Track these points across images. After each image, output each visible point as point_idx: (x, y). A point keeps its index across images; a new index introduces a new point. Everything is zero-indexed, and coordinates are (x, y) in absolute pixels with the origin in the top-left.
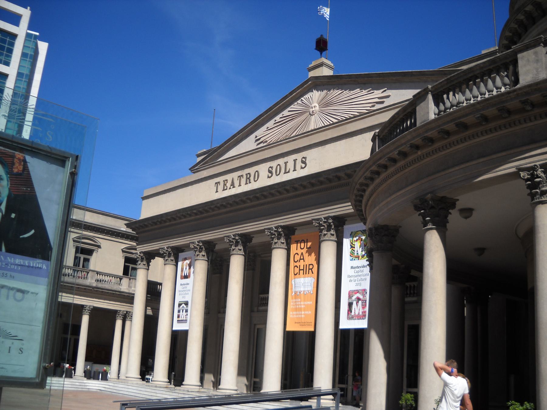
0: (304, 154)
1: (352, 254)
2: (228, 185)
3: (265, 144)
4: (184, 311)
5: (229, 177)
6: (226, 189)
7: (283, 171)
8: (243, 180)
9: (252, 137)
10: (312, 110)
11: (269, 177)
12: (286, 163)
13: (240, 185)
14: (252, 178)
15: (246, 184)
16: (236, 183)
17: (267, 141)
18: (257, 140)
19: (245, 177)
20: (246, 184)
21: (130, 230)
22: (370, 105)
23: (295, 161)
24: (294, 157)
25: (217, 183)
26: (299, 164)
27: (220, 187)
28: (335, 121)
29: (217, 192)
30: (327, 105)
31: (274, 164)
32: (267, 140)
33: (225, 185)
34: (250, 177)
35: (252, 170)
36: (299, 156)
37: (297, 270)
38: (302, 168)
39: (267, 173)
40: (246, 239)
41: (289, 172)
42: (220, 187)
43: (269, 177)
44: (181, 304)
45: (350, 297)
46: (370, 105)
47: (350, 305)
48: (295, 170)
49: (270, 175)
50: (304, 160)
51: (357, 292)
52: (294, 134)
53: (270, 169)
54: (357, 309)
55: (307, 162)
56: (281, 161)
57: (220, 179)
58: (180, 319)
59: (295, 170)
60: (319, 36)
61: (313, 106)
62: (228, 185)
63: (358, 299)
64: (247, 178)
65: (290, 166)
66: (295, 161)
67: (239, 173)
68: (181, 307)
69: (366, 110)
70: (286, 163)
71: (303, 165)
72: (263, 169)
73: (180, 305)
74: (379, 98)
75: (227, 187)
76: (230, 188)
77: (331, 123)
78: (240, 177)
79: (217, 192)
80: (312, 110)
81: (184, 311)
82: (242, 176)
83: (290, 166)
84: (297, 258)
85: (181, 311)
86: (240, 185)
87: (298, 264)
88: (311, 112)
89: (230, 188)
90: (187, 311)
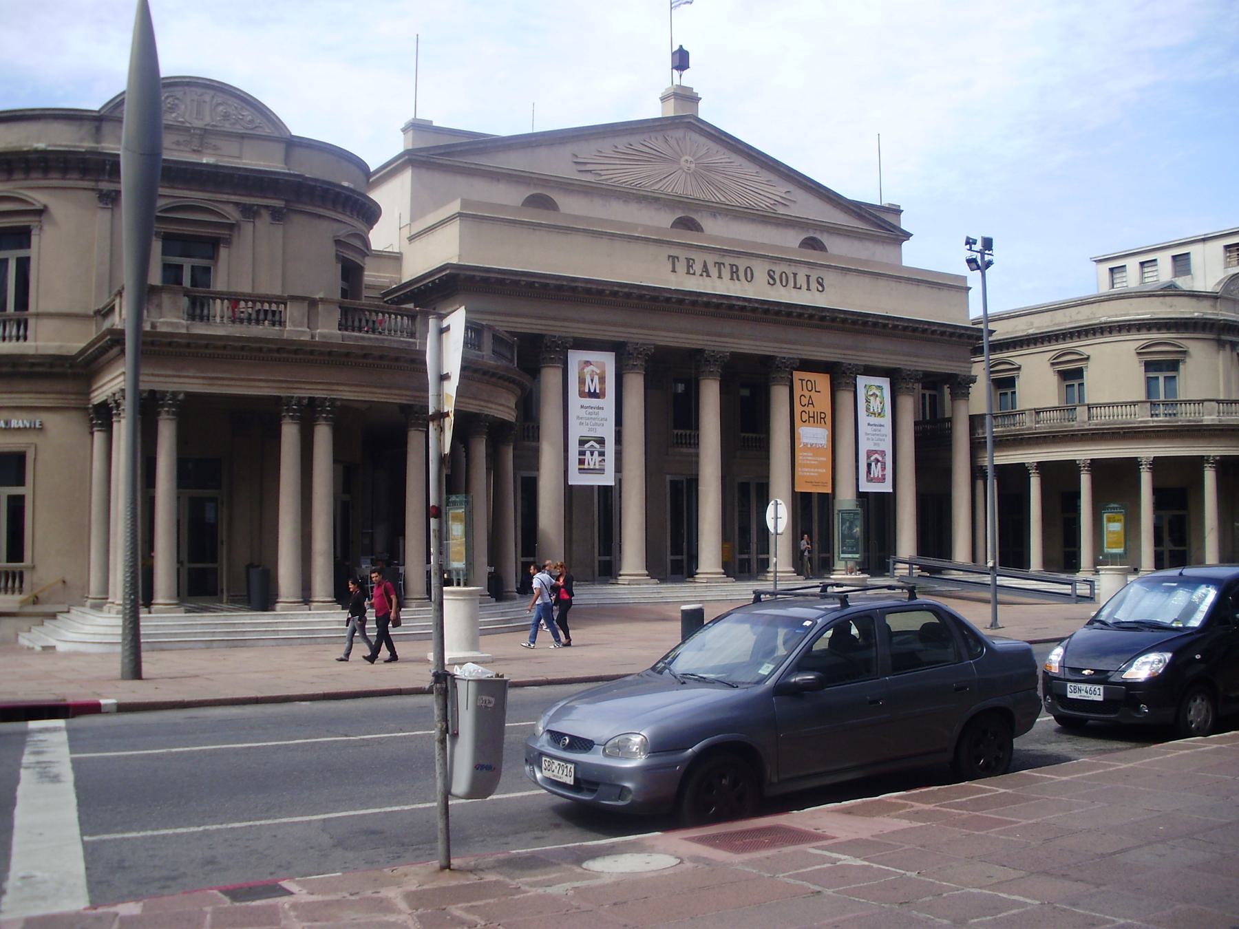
1: (868, 409)
2: (698, 268)
4: (596, 453)
5: (699, 259)
8: (726, 273)
9: (567, 151)
12: (795, 275)
13: (720, 277)
15: (732, 279)
16: (714, 272)
19: (728, 267)
20: (732, 279)
23: (808, 277)
26: (814, 285)
27: (681, 267)
29: (674, 271)
31: (778, 269)
33: (689, 267)
35: (742, 263)
37: (805, 417)
44: (588, 441)
45: (869, 457)
47: (869, 465)
48: (808, 289)
51: (876, 452)
54: (876, 471)
56: (784, 267)
57: (682, 254)
58: (586, 466)
59: (808, 289)
61: (690, 159)
62: (698, 268)
63: (878, 461)
64: (732, 273)
65: (801, 280)
66: (808, 277)
68: (587, 446)
70: (795, 275)
72: (760, 270)
73: (582, 442)
79: (674, 271)
81: (596, 453)
83: (801, 280)
84: (805, 401)
85: (588, 453)
86: (720, 277)
87: (805, 409)
90: (602, 454)
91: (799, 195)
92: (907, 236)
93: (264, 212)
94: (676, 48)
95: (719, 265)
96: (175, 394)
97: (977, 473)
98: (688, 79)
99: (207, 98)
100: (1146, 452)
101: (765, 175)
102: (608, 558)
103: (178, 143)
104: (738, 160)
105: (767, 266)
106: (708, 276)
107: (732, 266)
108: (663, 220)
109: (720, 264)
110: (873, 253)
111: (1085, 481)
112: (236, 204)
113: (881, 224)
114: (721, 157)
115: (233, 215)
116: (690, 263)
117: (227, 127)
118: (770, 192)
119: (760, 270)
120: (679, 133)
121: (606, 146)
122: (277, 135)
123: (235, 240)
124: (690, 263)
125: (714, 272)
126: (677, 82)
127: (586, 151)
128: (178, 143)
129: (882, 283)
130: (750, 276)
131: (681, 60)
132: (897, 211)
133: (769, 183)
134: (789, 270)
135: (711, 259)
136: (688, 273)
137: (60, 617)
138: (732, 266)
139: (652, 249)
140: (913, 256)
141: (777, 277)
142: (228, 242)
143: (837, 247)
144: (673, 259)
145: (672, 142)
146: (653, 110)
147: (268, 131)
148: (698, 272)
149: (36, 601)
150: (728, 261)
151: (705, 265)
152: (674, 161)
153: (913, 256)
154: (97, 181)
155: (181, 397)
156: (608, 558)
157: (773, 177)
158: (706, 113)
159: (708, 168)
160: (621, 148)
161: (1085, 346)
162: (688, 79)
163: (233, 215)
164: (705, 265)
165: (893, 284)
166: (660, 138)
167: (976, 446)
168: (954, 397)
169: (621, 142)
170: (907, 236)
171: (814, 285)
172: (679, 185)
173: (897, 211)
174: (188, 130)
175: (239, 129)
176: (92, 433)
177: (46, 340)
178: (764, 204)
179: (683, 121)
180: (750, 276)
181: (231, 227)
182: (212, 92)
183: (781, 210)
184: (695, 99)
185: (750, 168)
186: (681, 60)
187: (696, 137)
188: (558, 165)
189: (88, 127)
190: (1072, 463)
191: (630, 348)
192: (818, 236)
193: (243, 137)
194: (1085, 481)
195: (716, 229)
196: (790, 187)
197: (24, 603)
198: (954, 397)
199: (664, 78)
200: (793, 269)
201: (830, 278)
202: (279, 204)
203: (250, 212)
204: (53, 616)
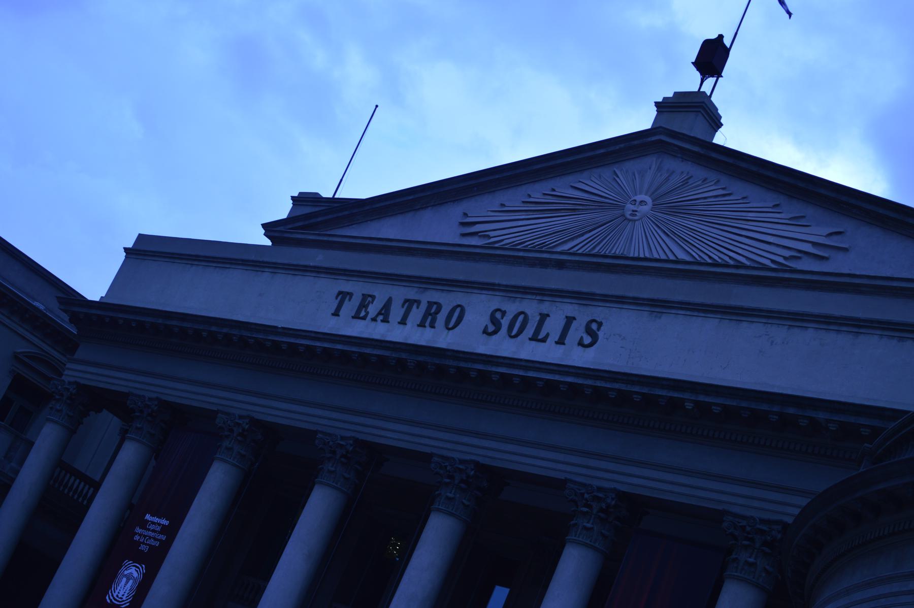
0: (599, 312)
2: (373, 309)
5: (381, 292)
6: (364, 318)
7: (530, 331)
8: (416, 314)
9: (455, 212)
10: (633, 207)
11: (485, 332)
13: (403, 322)
14: (441, 318)
15: (422, 325)
16: (396, 312)
17: (489, 237)
18: (463, 224)
19: (424, 306)
20: (422, 325)
21: (66, 317)
22: (787, 253)
23: (570, 320)
24: (569, 309)
25: (344, 296)
26: (577, 332)
27: (349, 307)
28: (682, 256)
29: (336, 314)
30: (675, 209)
31: (512, 308)
32: (492, 234)
33: (363, 305)
34: (438, 311)
35: (447, 300)
36: (583, 315)
38: (581, 344)
39: (485, 320)
40: (369, 456)
41: (543, 340)
42: (349, 307)
43: (485, 332)
46: (787, 253)
48: (561, 342)
49: (491, 328)
50: (594, 326)
52: (566, 247)
53: (498, 315)
55: (601, 334)
57: (357, 288)
59: (561, 342)
60: (714, 36)
61: (639, 198)
62: (373, 309)
64: (427, 313)
65: (553, 326)
66: (570, 320)
67: (411, 293)
69: (773, 261)
70: (544, 317)
71: (587, 340)
72: (479, 309)
74: (814, 244)
75: (367, 313)
76: (374, 320)
77: (672, 258)
78: (410, 304)
80: (633, 207)
82: (418, 302)
83: (553, 326)
88: (628, 214)
89: (374, 320)
95: (410, 304)
105: (493, 302)
106: (386, 320)
107: (430, 304)
133: (796, 221)
134: (532, 308)
135: (399, 293)
136: (356, 317)
138: (430, 304)
141: (505, 322)
144: (344, 296)
151: (389, 303)
160: (537, 196)
164: (389, 303)
165: (778, 332)
169: (537, 191)
171: (577, 332)
185: (760, 199)
186: (712, 57)
200: (545, 308)
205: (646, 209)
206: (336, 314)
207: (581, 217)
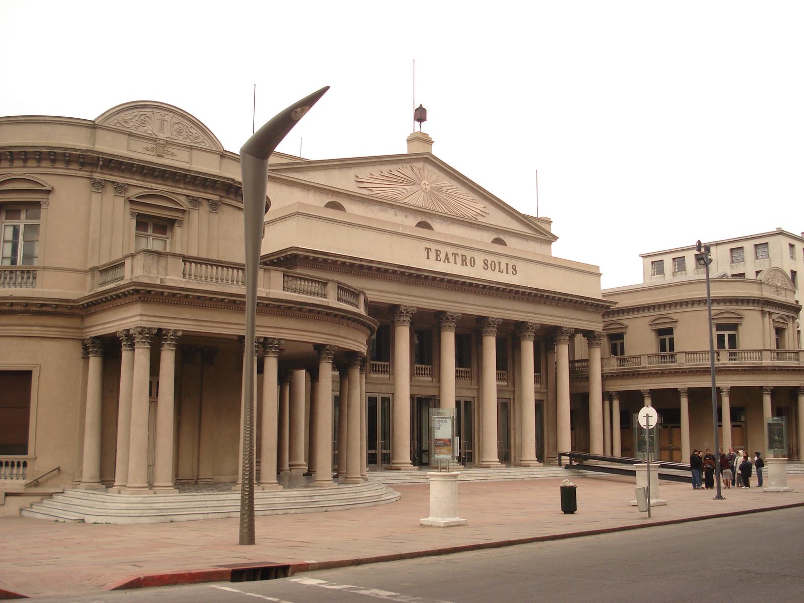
2: (442, 256)
3: (371, 193)
5: (443, 250)
8: (459, 260)
9: (352, 173)
12: (500, 263)
13: (455, 263)
14: (468, 261)
16: (452, 259)
23: (507, 264)
26: (510, 270)
27: (433, 255)
29: (428, 258)
31: (490, 258)
33: (437, 256)
35: (469, 254)
36: (511, 262)
52: (406, 201)
61: (427, 183)
62: (442, 256)
65: (503, 267)
70: (500, 263)
72: (479, 259)
83: (503, 267)
86: (455, 263)
91: (491, 209)
92: (555, 238)
93: (205, 202)
94: (417, 106)
95: (455, 255)
96: (176, 331)
97: (607, 396)
98: (426, 127)
99: (167, 118)
100: (726, 383)
101: (471, 196)
102: (373, 452)
103: (147, 149)
104: (455, 185)
108: (411, 221)
109: (455, 255)
110: (533, 249)
111: (684, 402)
112: (188, 196)
113: (539, 231)
114: (445, 181)
115: (185, 204)
116: (438, 253)
117: (180, 140)
118: (474, 207)
119: (479, 259)
120: (420, 165)
121: (376, 171)
122: (214, 149)
123: (185, 222)
124: (438, 253)
125: (452, 259)
126: (417, 129)
127: (364, 173)
128: (147, 149)
129: (550, 270)
130: (473, 263)
131: (420, 115)
132: (549, 222)
134: (496, 259)
135: (450, 250)
137: (54, 496)
139: (415, 242)
140: (558, 250)
141: (489, 264)
142: (181, 223)
143: (513, 244)
144: (428, 250)
145: (416, 170)
146: (402, 148)
147: (208, 145)
148: (443, 259)
149: (36, 483)
150: (460, 252)
152: (417, 183)
153: (558, 250)
154: (91, 172)
155: (180, 334)
156: (373, 452)
157: (476, 197)
158: (437, 151)
159: (438, 190)
161: (674, 313)
162: (426, 127)
163: (185, 204)
166: (409, 167)
167: (605, 378)
168: (590, 345)
170: (555, 238)
172: (418, 199)
173: (549, 222)
174: (155, 140)
175: (188, 142)
176: (86, 358)
177: (50, 287)
178: (469, 214)
179: (420, 156)
180: (473, 263)
181: (183, 211)
182: (172, 115)
183: (480, 219)
184: (430, 142)
185: (463, 190)
186: (420, 115)
187: (429, 167)
188: (343, 181)
189: (86, 132)
190: (675, 391)
191: (402, 308)
192: (502, 237)
193: (191, 148)
194: (684, 402)
195: (440, 228)
196: (486, 204)
197: (28, 486)
198: (590, 345)
199: (409, 126)
201: (520, 265)
202: (216, 198)
203: (195, 202)
204: (50, 495)
205: (428, 187)
206: (428, 258)
207: (406, 187)
